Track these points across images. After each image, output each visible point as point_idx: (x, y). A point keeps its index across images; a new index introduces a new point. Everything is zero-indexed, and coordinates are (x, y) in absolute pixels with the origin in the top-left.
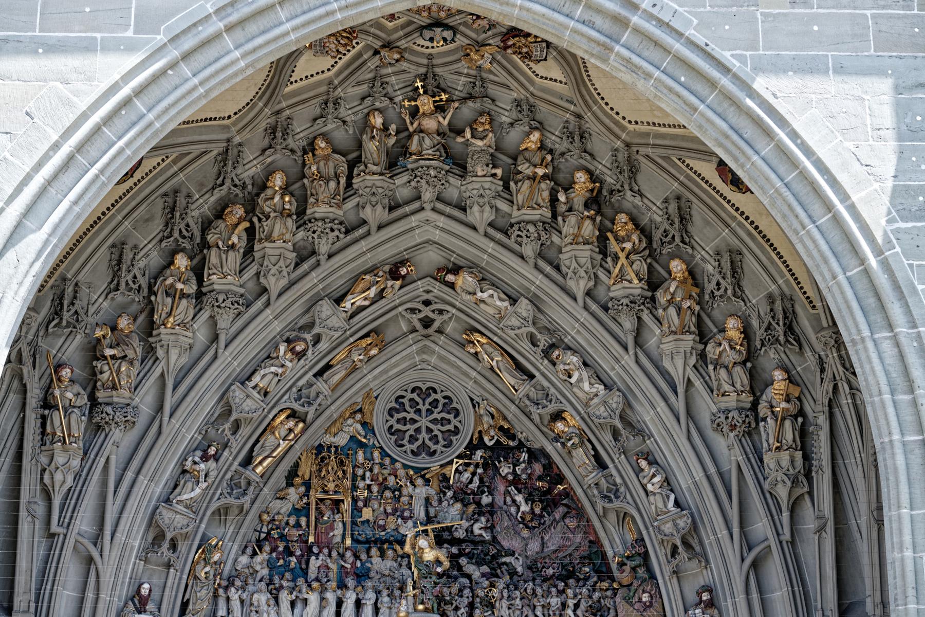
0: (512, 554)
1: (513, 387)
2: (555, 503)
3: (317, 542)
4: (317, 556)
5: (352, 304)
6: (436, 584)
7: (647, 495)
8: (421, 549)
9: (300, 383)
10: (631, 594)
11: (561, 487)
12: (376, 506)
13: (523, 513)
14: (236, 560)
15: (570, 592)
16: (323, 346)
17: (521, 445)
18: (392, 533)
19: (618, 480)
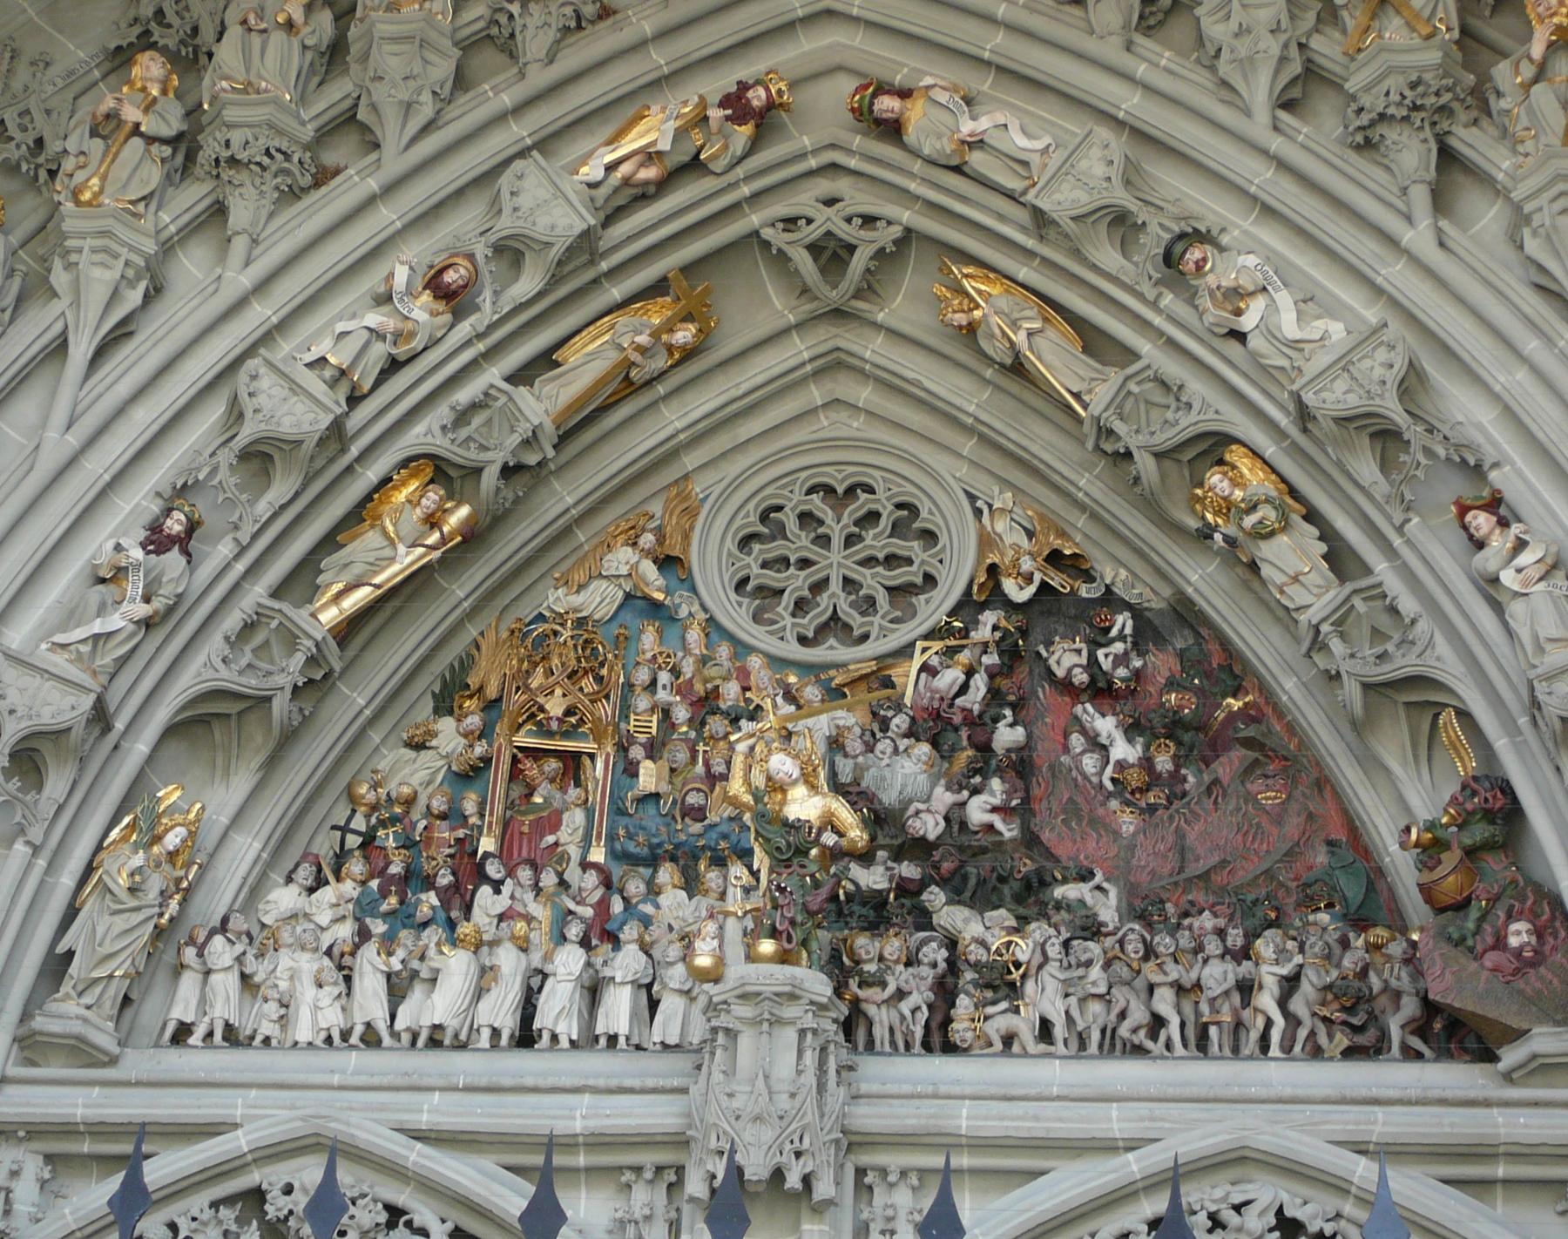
0: (1085, 876)
1: (1077, 396)
2: (1215, 747)
3: (504, 853)
4: (497, 886)
5: (611, 168)
6: (817, 885)
7: (1498, 608)
8: (777, 787)
9: (464, 395)
10: (1471, 925)
11: (1235, 704)
12: (682, 756)
13: (1121, 765)
14: (255, 890)
15: (1265, 946)
16: (526, 285)
17: (1110, 599)
18: (724, 828)
19: (1408, 605)
